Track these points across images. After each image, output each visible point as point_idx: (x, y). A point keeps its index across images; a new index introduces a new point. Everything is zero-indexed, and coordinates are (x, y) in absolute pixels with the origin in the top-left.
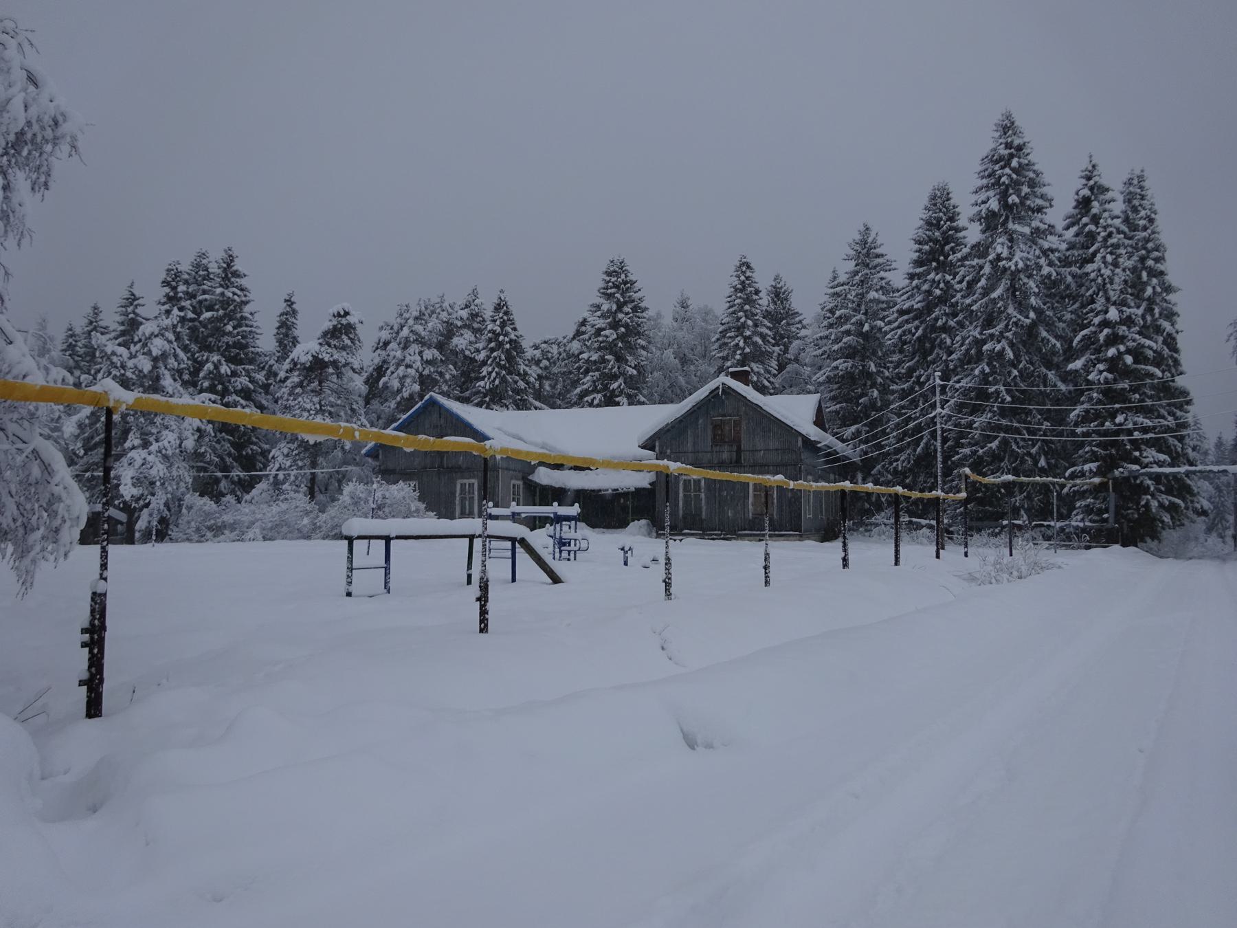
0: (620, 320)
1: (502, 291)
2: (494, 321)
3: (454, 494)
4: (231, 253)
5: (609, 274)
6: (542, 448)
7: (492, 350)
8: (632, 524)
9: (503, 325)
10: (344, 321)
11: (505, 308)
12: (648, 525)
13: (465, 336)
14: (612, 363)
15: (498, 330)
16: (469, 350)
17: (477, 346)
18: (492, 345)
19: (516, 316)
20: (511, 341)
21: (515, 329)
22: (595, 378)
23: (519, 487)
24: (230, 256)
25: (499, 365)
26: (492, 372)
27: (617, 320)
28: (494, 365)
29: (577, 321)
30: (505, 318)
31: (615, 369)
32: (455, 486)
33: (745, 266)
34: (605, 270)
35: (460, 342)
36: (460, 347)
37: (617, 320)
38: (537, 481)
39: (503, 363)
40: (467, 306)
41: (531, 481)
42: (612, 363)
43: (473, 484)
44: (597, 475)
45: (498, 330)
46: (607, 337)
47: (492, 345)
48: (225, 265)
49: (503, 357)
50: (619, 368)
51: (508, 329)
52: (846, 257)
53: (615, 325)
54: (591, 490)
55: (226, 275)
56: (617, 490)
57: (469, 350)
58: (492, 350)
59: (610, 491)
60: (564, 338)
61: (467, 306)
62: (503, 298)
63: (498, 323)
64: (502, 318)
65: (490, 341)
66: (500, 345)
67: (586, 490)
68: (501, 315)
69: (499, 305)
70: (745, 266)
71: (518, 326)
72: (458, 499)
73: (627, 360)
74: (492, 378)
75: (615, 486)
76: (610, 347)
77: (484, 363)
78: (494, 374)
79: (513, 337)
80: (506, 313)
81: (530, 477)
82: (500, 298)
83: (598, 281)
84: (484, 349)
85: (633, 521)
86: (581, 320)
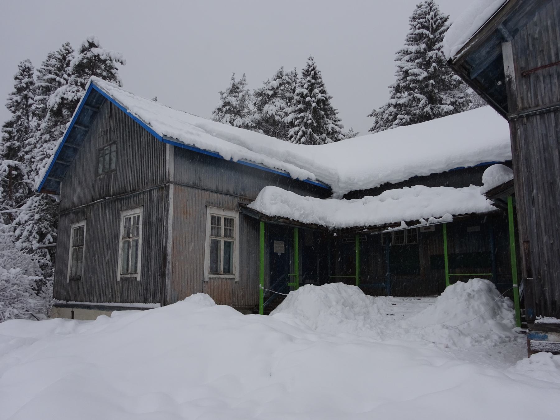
0: (431, 58)
1: (311, 59)
2: (302, 86)
3: (117, 236)
4: (67, 47)
5: (414, 19)
6: (286, 161)
7: (300, 111)
8: (449, 289)
9: (311, 88)
10: (89, 55)
12: (490, 290)
13: (277, 103)
14: (423, 102)
15: (306, 92)
16: (280, 115)
17: (286, 110)
18: (300, 106)
19: (325, 78)
20: (318, 102)
22: (404, 121)
23: (232, 220)
24: (66, 50)
25: (306, 125)
26: (298, 132)
27: (427, 59)
28: (302, 125)
30: (313, 81)
31: (428, 109)
32: (119, 221)
35: (271, 108)
36: (270, 113)
39: (309, 121)
40: (279, 77)
41: (252, 211)
42: (423, 102)
43: (138, 217)
45: (306, 92)
46: (416, 75)
47: (300, 106)
48: (60, 57)
49: (310, 116)
50: (432, 109)
51: (316, 91)
53: (426, 65)
54: (370, 227)
55: (62, 66)
56: (418, 222)
57: (280, 115)
58: (300, 111)
59: (403, 226)
60: (380, 108)
61: (279, 77)
62: (311, 64)
63: (306, 86)
64: (309, 81)
65: (299, 102)
66: (308, 104)
67: (362, 228)
68: (309, 78)
69: (307, 71)
71: (327, 88)
72: (121, 245)
73: (442, 99)
74: (298, 137)
75: (411, 214)
76: (422, 86)
77: (292, 124)
78: (300, 133)
79: (320, 96)
80: (315, 77)
81: (249, 206)
84: (292, 112)
85: (453, 281)
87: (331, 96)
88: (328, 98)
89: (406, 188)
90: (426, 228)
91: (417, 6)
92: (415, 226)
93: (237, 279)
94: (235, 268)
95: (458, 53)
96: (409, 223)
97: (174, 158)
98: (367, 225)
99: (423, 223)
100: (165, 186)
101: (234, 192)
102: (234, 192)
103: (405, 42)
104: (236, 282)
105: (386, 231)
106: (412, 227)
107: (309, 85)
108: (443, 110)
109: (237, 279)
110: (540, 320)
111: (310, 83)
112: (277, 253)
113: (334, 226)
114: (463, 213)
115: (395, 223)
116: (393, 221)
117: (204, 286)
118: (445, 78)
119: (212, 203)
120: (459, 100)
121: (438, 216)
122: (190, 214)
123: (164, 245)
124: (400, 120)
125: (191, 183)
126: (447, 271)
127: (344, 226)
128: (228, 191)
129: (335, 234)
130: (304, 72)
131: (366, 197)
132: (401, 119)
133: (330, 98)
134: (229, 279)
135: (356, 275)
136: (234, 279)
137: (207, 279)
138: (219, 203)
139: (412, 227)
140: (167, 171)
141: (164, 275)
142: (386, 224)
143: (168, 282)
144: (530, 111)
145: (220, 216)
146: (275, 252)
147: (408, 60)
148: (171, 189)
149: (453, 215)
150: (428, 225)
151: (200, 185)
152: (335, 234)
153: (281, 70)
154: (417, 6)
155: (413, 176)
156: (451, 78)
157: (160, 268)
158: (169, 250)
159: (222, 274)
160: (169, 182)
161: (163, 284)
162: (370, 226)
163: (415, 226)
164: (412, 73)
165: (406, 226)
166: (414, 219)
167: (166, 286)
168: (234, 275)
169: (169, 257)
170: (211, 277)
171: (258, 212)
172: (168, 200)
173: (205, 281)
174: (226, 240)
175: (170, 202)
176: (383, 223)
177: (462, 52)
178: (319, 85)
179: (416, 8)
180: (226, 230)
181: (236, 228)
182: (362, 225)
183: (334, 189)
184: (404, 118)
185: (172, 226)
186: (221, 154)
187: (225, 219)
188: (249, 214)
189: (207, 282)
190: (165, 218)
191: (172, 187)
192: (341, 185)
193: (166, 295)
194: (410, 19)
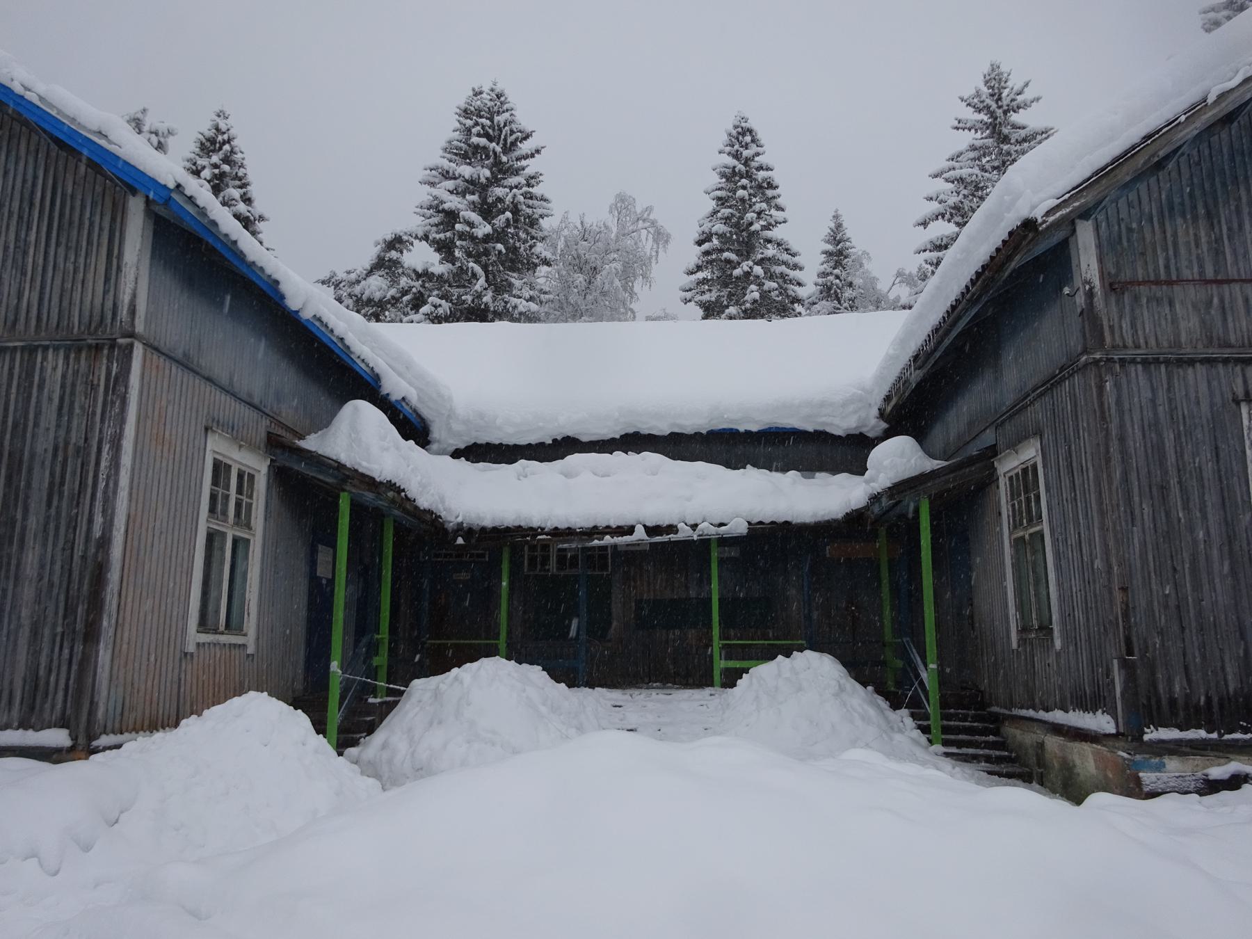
0: (500, 200)
11: (227, 147)
21: (247, 200)
27: (490, 200)
29: (380, 238)
30: (226, 168)
33: (743, 136)
34: (463, 106)
37: (490, 200)
38: (344, 458)
44: (568, 475)
46: (471, 224)
52: (956, 123)
53: (487, 211)
54: (556, 532)
56: (672, 529)
59: (640, 533)
60: (349, 273)
62: (223, 127)
63: (207, 173)
64: (215, 166)
67: (534, 531)
68: (215, 159)
69: (212, 141)
70: (743, 136)
71: (253, 191)
81: (311, 443)
82: (217, 129)
83: (447, 128)
86: (389, 237)
87: (266, 215)
88: (257, 217)
89: (619, 455)
90: (687, 543)
91: (474, 90)
92: (665, 538)
93: (251, 650)
94: (248, 614)
95: (1048, 213)
96: (652, 530)
97: (151, 265)
98: (549, 526)
99: (684, 533)
100: (113, 345)
101: (261, 402)
102: (261, 402)
103: (441, 153)
104: (248, 656)
105: (596, 542)
106: (658, 539)
107: (215, 176)
108: (515, 307)
109: (251, 650)
110: (1151, 735)
111: (217, 171)
112: (321, 578)
113: (460, 519)
114: (767, 521)
115: (619, 527)
116: (614, 524)
117: (184, 665)
118: (520, 248)
119: (218, 421)
120: (542, 296)
121: (717, 522)
122: (170, 443)
123: (97, 532)
124: (433, 309)
125: (179, 354)
126: (716, 632)
127: (488, 523)
128: (250, 395)
129: (460, 541)
130: (204, 141)
131: (523, 462)
132: (435, 307)
133: (261, 218)
134: (235, 645)
135: (499, 640)
136: (244, 646)
137: (191, 648)
138: (231, 424)
139: (658, 539)
140: (126, 298)
141: (91, 634)
142: (595, 527)
143: (104, 655)
144: (1129, 354)
145: (229, 462)
146: (318, 574)
147: (451, 189)
148: (137, 356)
149: (749, 523)
150: (695, 538)
151: (198, 361)
152: (460, 541)
153: (140, 116)
154: (474, 90)
155: (631, 431)
156: (530, 250)
157: (69, 611)
158: (116, 552)
159: (222, 633)
160: (132, 335)
161: (86, 664)
162: (556, 528)
163: (665, 538)
164: (467, 218)
165: (646, 537)
166: (665, 522)
167: (99, 670)
168: (245, 635)
169: (114, 576)
170: (201, 641)
171: (340, 466)
172: (126, 392)
173: (186, 654)
174: (238, 534)
175: (131, 399)
176: (591, 525)
177: (1058, 215)
178: (237, 183)
179: (471, 93)
180: (238, 505)
181: (258, 500)
182: (535, 524)
183: (436, 432)
184: (440, 305)
185: (129, 473)
186: (283, 287)
187: (240, 476)
188: (302, 467)
189: (192, 654)
190: (106, 448)
191: (138, 350)
192: (456, 427)
193: (96, 700)
194: (458, 111)
